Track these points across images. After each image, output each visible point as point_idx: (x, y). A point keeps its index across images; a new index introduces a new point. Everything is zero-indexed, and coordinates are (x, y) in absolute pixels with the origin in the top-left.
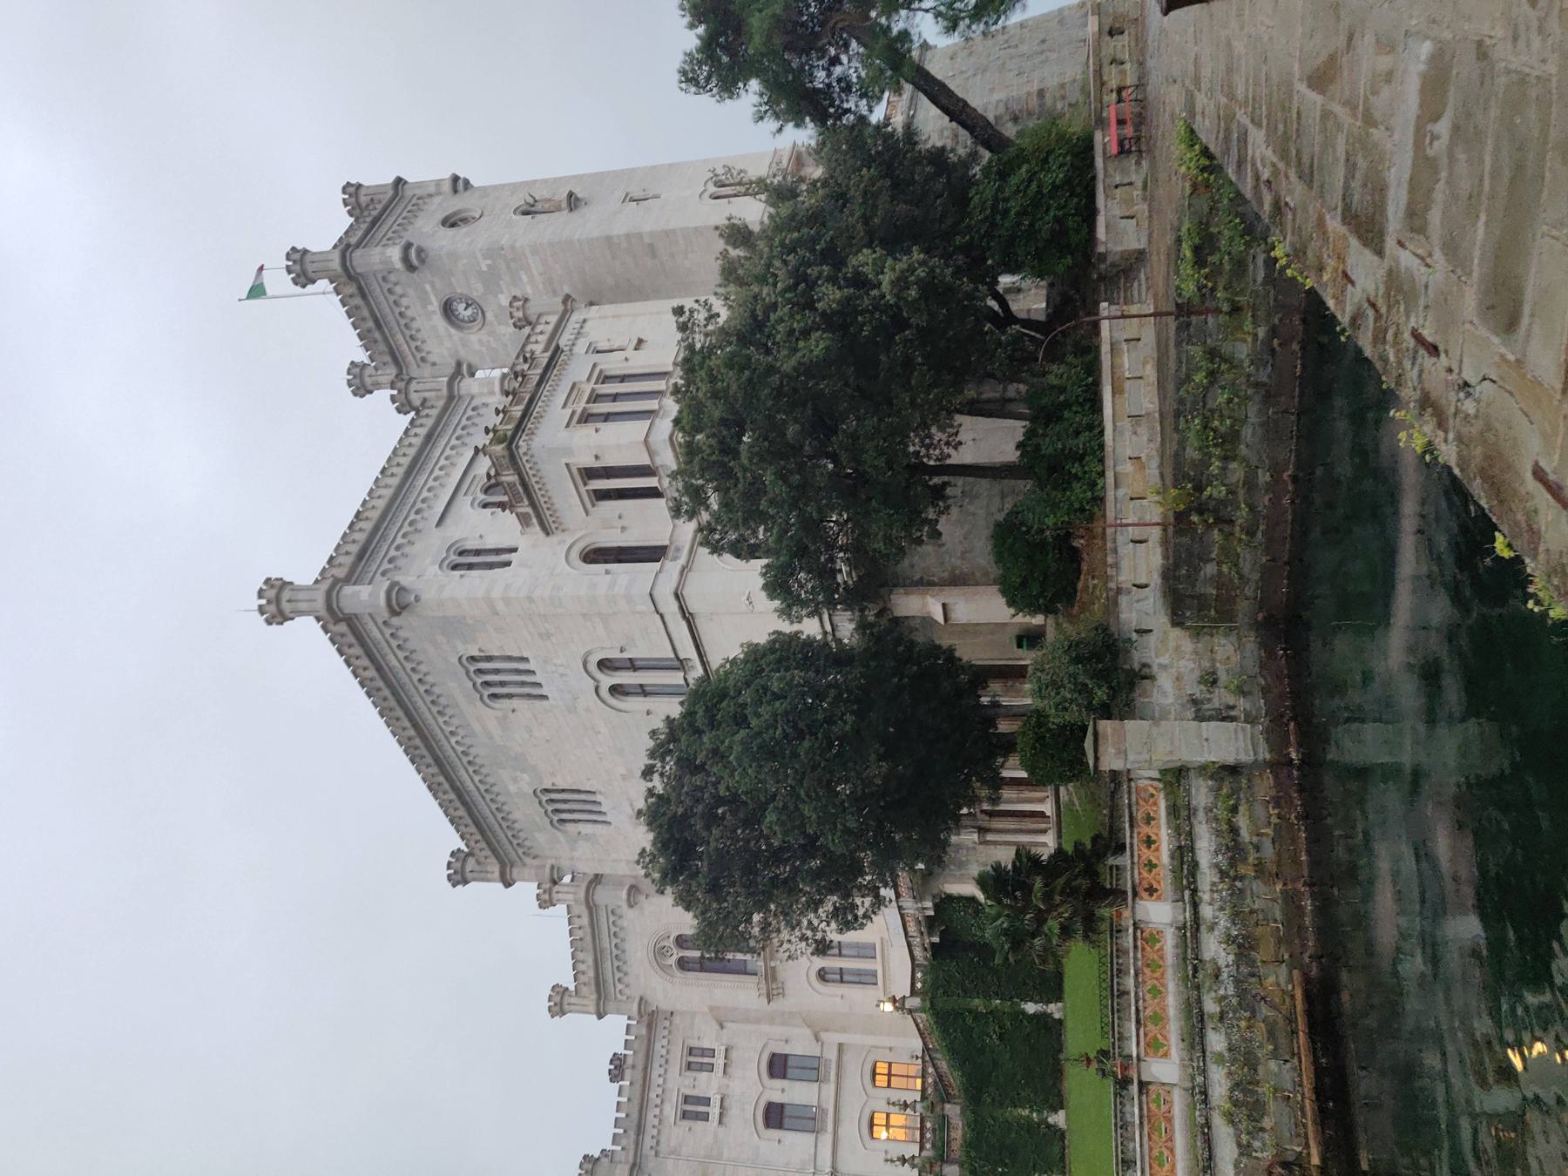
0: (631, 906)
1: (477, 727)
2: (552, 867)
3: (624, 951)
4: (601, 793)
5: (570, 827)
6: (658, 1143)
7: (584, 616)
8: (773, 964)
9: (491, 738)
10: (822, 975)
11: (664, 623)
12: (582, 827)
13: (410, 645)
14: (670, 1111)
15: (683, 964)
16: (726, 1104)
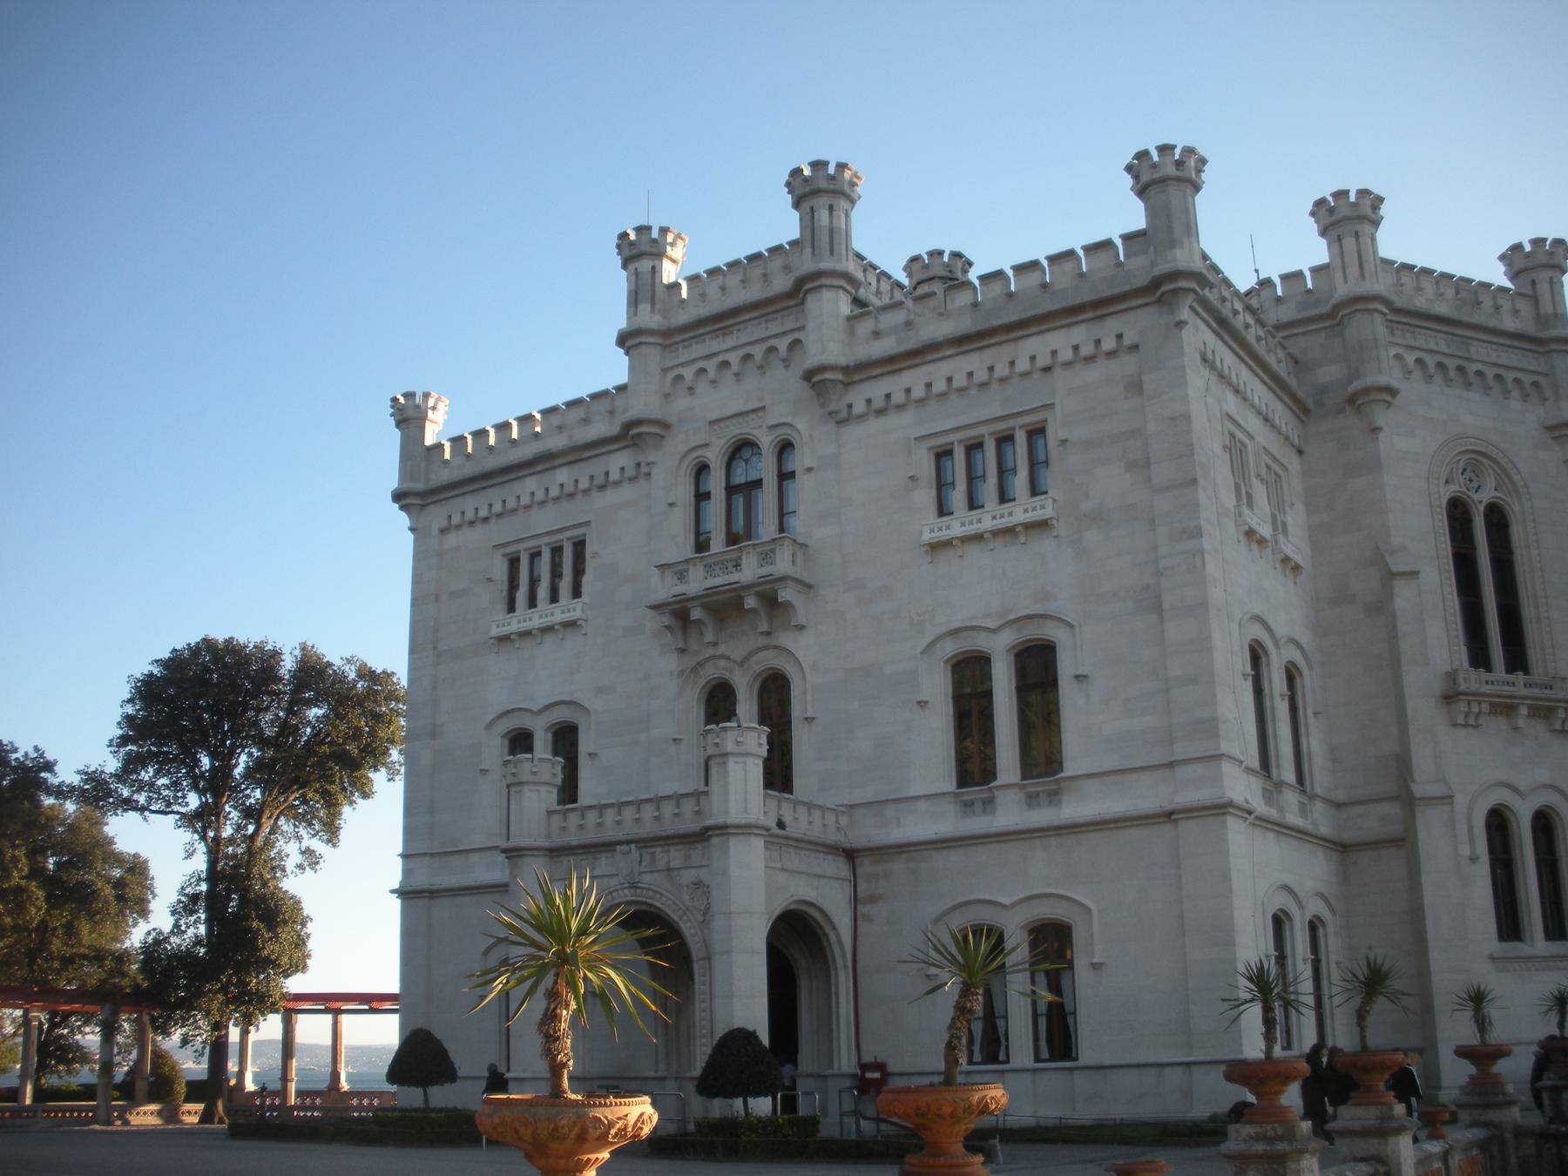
0: (1550, 428)
3: (1468, 385)
8: (1524, 711)
10: (1498, 823)
15: (1458, 513)
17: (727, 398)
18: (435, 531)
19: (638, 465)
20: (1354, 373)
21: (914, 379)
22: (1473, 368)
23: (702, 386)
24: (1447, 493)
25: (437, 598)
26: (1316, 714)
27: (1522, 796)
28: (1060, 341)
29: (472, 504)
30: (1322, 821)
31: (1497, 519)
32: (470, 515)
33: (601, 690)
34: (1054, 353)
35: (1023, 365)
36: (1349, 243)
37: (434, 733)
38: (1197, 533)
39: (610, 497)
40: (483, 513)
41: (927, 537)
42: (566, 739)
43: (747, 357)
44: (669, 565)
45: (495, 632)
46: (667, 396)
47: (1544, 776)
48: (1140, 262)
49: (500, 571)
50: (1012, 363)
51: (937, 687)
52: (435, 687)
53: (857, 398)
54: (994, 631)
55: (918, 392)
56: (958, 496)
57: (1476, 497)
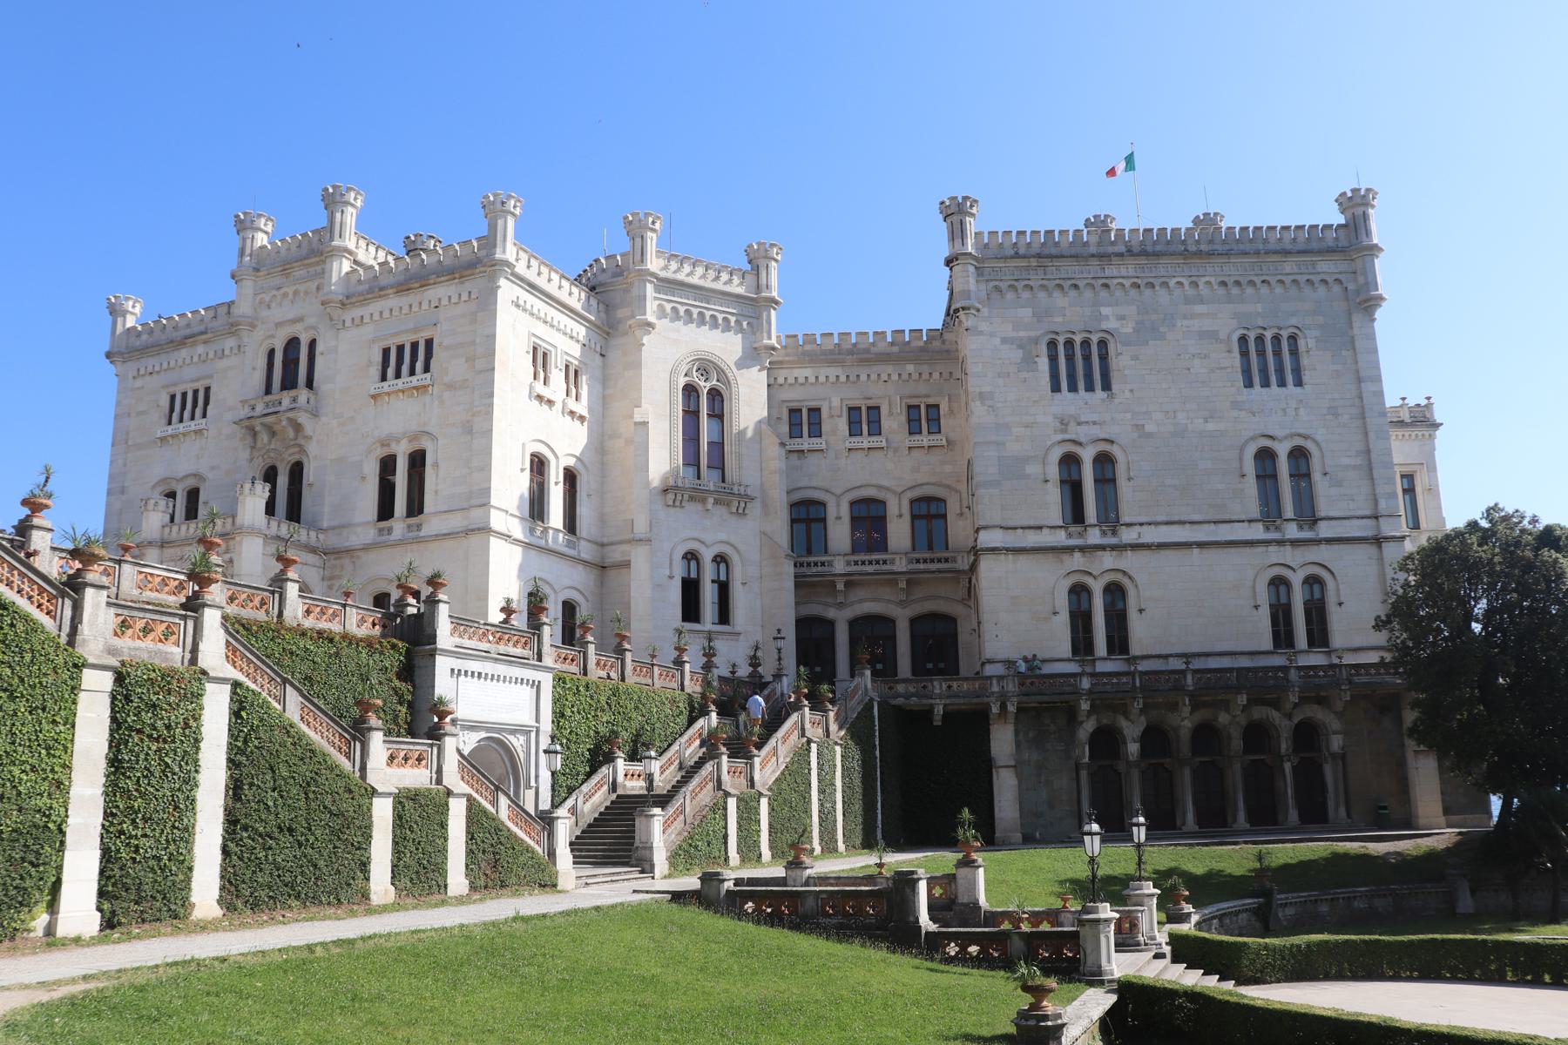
1: (1199, 309)
2: (978, 310)
4: (1111, 397)
5: (1044, 349)
6: (518, 306)
7: (1368, 451)
9: (1185, 317)
11: (1362, 518)
12: (1044, 363)
13: (1307, 290)
14: (541, 329)
15: (690, 391)
16: (545, 407)
17: (287, 311)
18: (130, 376)
19: (239, 346)
20: (633, 316)
21: (374, 307)
22: (708, 314)
23: (273, 305)
24: (682, 381)
25: (129, 415)
26: (589, 495)
27: (707, 546)
28: (440, 292)
29: (151, 362)
30: (586, 551)
31: (715, 394)
32: (150, 369)
33: (213, 468)
34: (440, 299)
35: (425, 306)
36: (638, 240)
37: (122, 491)
38: (491, 395)
39: (225, 363)
40: (157, 369)
41: (373, 392)
42: (193, 495)
43: (296, 293)
44: (246, 401)
45: (159, 435)
46: (255, 309)
47: (723, 537)
48: (483, 253)
49: (165, 402)
50: (420, 303)
51: (372, 470)
52: (125, 465)
53: (348, 316)
54: (398, 441)
55: (376, 317)
56: (391, 371)
57: (702, 384)
